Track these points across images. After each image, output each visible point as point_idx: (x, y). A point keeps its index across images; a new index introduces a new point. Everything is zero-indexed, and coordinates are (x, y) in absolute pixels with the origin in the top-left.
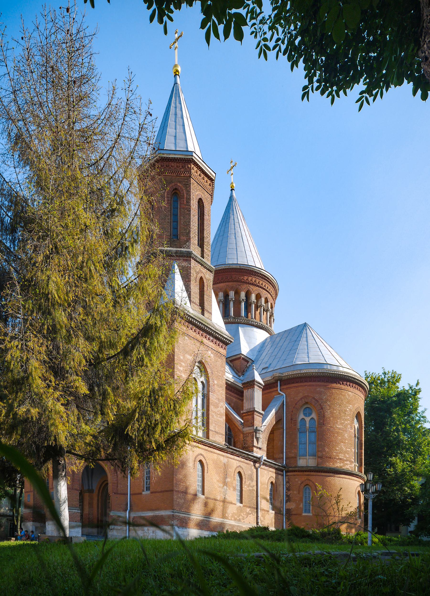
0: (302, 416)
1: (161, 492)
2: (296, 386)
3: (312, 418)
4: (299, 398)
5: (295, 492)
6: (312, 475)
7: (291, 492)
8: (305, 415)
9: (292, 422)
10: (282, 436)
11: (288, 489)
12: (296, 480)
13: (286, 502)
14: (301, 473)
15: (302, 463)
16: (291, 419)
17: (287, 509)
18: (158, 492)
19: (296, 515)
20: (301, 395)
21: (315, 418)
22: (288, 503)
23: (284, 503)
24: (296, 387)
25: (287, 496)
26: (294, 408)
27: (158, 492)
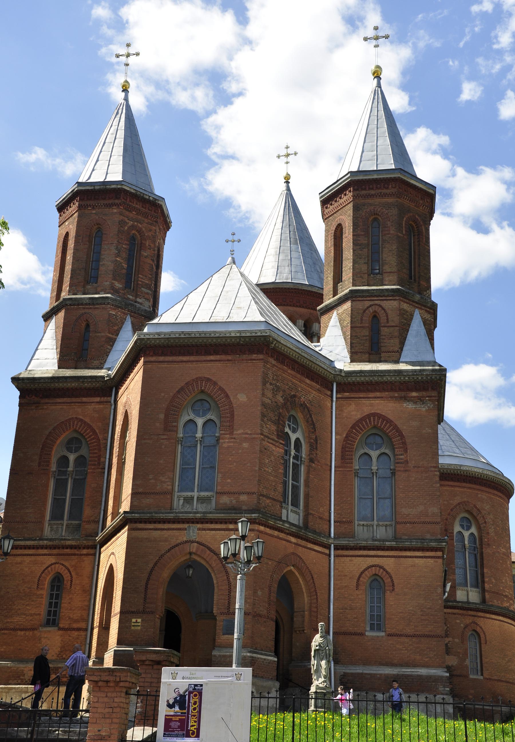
0: (457, 528)
1: (414, 636)
3: (472, 534)
6: (492, 619)
7: (450, 639)
8: (462, 526)
9: (447, 534)
12: (458, 621)
14: (464, 612)
15: (461, 595)
18: (407, 636)
19: (460, 676)
21: (476, 534)
24: (452, 486)
27: (407, 636)
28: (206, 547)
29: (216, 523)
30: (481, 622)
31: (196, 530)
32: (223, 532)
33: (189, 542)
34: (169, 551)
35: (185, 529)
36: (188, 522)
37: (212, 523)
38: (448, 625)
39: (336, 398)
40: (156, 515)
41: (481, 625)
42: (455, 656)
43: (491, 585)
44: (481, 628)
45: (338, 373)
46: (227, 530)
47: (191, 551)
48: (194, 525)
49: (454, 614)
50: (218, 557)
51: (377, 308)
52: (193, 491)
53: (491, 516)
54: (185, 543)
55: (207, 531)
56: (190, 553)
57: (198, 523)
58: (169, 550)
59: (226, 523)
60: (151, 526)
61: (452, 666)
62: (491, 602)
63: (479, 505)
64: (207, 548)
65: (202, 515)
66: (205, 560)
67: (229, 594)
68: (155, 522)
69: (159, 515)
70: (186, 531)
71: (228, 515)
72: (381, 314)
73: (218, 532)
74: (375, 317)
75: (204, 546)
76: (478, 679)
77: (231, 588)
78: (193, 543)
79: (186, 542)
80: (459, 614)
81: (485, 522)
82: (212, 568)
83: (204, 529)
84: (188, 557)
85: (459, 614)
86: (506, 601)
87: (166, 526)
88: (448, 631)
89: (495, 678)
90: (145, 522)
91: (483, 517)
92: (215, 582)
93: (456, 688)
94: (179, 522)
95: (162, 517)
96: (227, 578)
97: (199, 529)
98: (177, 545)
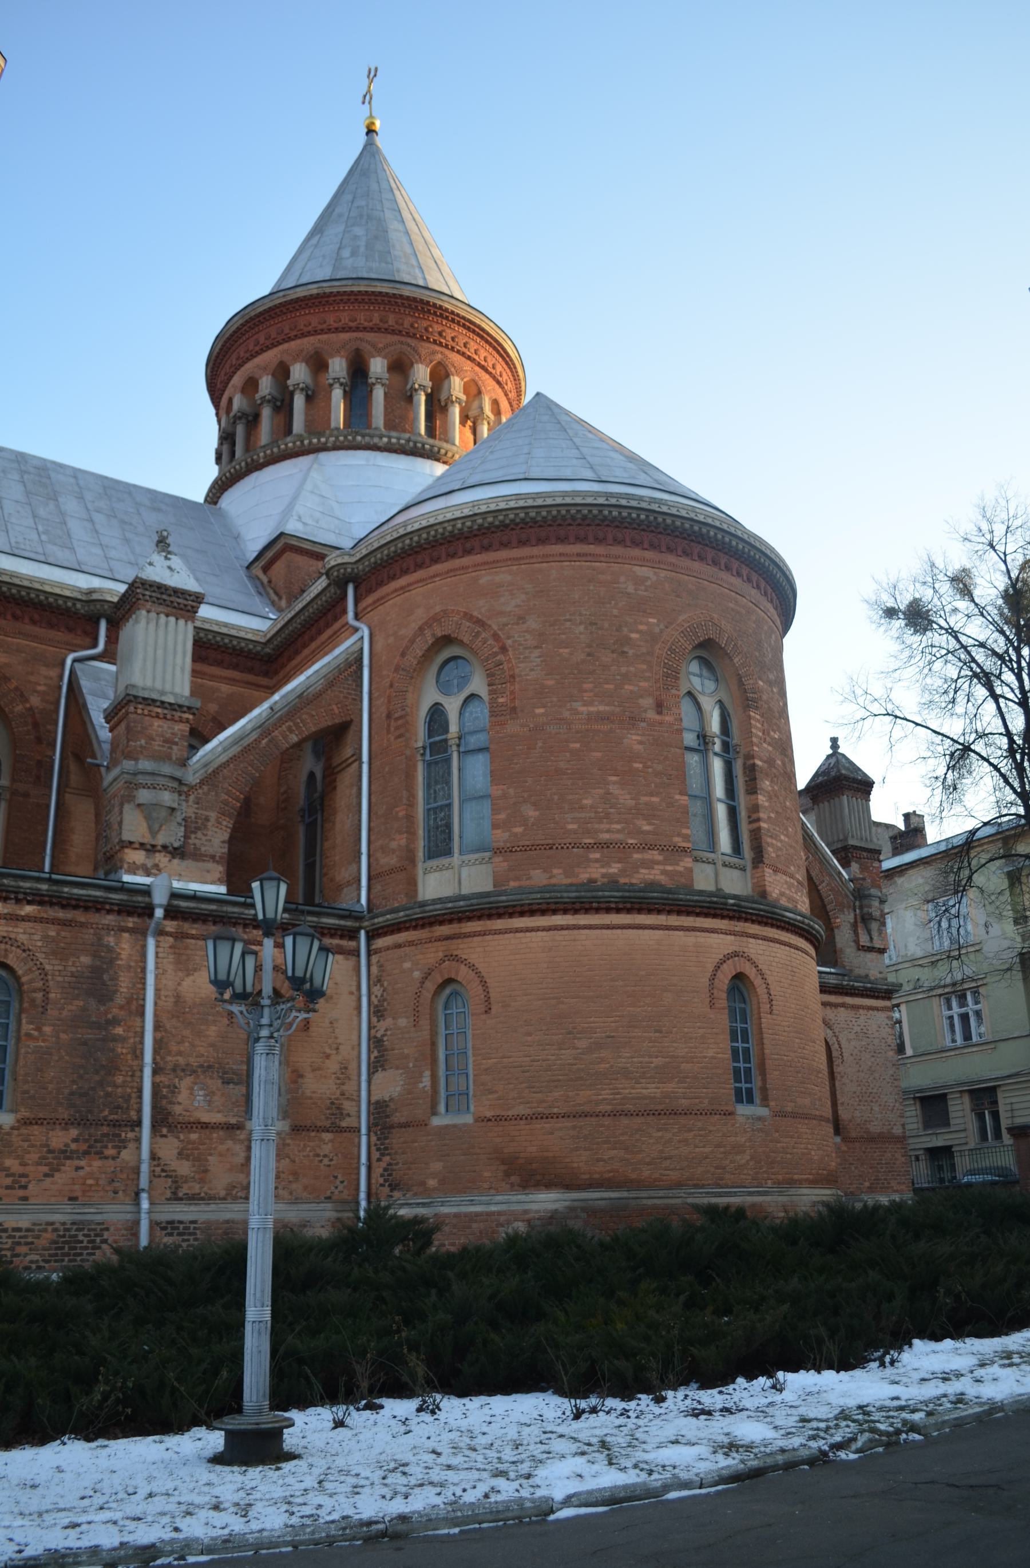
2: (402, 588)
4: (415, 626)
5: (403, 1022)
7: (388, 1022)
8: (445, 688)
9: (389, 726)
10: (354, 790)
11: (378, 1012)
13: (374, 1067)
16: (389, 716)
17: (377, 1102)
20: (420, 615)
22: (379, 1076)
23: (364, 1077)
25: (376, 1042)
26: (397, 669)
30: (473, 951)
38: (386, 984)
41: (474, 958)
42: (397, 1068)
43: (519, 830)
44: (472, 967)
49: (399, 946)
53: (533, 623)
61: (391, 1099)
62: (517, 879)
63: (480, 608)
76: (455, 1126)
80: (411, 943)
81: (504, 649)
85: (411, 943)
86: (597, 861)
88: (385, 1000)
89: (522, 1110)
91: (496, 637)
93: (397, 1164)
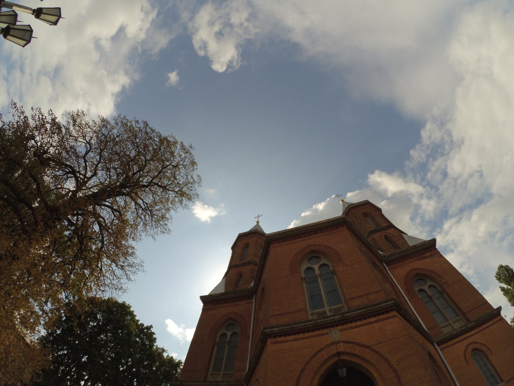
28: (353, 344)
29: (356, 321)
31: (338, 332)
32: (366, 326)
33: (334, 344)
34: (314, 357)
35: (327, 334)
36: (327, 327)
37: (351, 322)
39: (389, 269)
40: (295, 326)
45: (383, 255)
46: (369, 324)
47: (339, 351)
48: (333, 328)
50: (370, 349)
51: (385, 234)
52: (323, 306)
54: (330, 346)
55: (350, 330)
56: (338, 354)
57: (337, 325)
58: (315, 355)
59: (365, 318)
60: (292, 337)
64: (356, 344)
65: (340, 316)
66: (358, 356)
67: (398, 381)
68: (294, 334)
69: (298, 325)
70: (328, 335)
71: (366, 310)
72: (388, 234)
73: (362, 327)
74: (386, 238)
75: (351, 343)
77: (398, 374)
78: (339, 343)
79: (331, 344)
82: (368, 362)
83: (346, 329)
84: (336, 359)
87: (307, 335)
90: (285, 335)
92: (375, 375)
94: (318, 329)
95: (301, 328)
96: (390, 366)
97: (341, 330)
98: (322, 350)
